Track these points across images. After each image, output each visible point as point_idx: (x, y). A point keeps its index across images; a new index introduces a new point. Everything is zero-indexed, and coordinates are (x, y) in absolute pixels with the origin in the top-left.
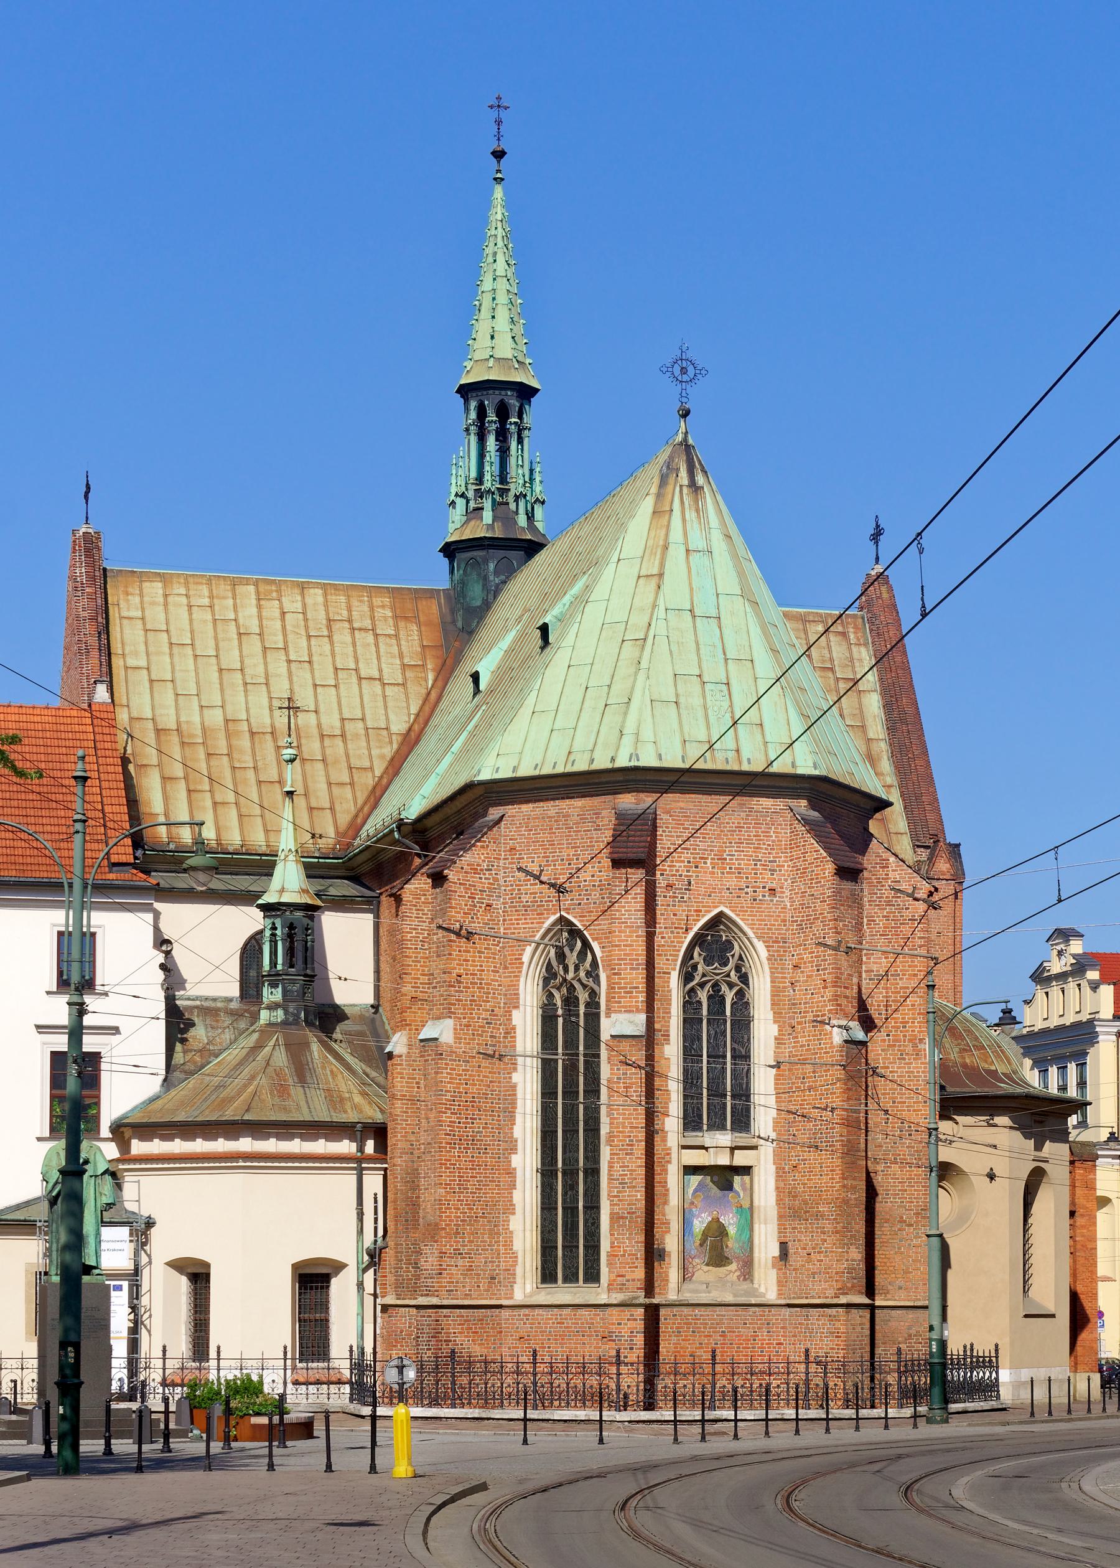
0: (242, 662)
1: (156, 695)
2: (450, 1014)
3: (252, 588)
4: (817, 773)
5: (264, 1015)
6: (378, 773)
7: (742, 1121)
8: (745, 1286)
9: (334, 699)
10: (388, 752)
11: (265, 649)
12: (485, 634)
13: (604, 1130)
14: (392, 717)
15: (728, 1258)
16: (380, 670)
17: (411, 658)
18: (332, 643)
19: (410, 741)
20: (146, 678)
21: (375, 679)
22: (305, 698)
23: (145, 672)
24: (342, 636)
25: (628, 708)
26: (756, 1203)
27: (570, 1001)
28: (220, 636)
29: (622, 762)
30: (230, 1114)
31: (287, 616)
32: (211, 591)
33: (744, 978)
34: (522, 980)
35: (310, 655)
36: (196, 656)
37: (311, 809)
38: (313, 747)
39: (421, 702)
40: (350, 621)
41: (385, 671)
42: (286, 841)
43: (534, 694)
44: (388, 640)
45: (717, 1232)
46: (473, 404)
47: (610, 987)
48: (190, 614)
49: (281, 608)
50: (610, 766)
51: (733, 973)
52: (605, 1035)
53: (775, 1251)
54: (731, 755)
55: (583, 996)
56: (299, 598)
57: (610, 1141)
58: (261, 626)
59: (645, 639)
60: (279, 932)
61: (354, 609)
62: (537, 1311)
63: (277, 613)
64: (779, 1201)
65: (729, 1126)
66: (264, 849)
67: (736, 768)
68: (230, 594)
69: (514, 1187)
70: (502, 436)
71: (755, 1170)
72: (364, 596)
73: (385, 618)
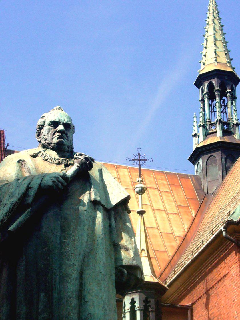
10: (176, 244)
14: (175, 229)
16: (164, 206)
17: (181, 202)
21: (162, 210)
44: (167, 194)
60: (137, 305)
61: (145, 179)
72: (150, 174)
73: (164, 185)
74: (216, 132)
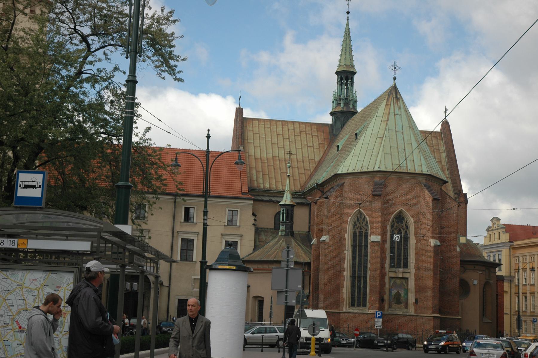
0: (278, 142)
1: (255, 150)
2: (328, 234)
3: (281, 123)
4: (428, 173)
5: (280, 233)
6: (312, 171)
7: (406, 265)
8: (406, 310)
9: (301, 152)
10: (314, 166)
11: (284, 139)
12: (341, 136)
13: (369, 266)
14: (316, 157)
15: (401, 302)
16: (313, 145)
18: (301, 137)
19: (320, 163)
20: (253, 145)
22: (293, 151)
23: (253, 144)
24: (303, 136)
25: (378, 155)
26: (409, 287)
27: (361, 233)
28: (272, 135)
29: (376, 169)
30: (270, 258)
31: (290, 130)
32: (270, 124)
33: (407, 227)
34: (348, 226)
35: (295, 140)
36: (266, 140)
37: (294, 180)
38: (295, 164)
39: (323, 153)
40: (306, 132)
41: (314, 145)
42: (287, 188)
43: (353, 151)
45: (398, 295)
46: (339, 76)
47: (371, 229)
48: (265, 129)
49: (288, 128)
50: (373, 170)
51: (404, 226)
52: (369, 242)
53: (414, 301)
54: (405, 168)
55: (364, 231)
56: (293, 126)
57: (370, 270)
58: (283, 133)
59: (383, 137)
60: (284, 211)
62: (349, 314)
63: (287, 129)
64: (415, 287)
65: (402, 266)
66: (281, 190)
67: (406, 171)
68: (275, 124)
69: (344, 280)
70: (347, 85)
71: (409, 279)
73: (315, 131)
74: (341, 103)
